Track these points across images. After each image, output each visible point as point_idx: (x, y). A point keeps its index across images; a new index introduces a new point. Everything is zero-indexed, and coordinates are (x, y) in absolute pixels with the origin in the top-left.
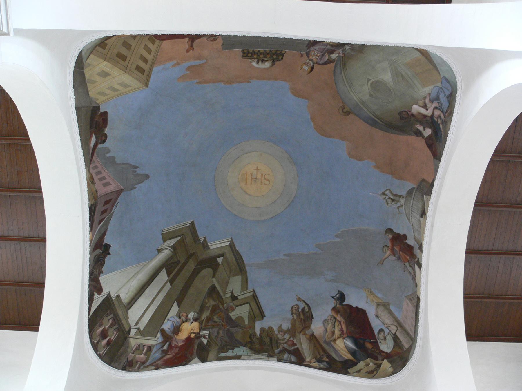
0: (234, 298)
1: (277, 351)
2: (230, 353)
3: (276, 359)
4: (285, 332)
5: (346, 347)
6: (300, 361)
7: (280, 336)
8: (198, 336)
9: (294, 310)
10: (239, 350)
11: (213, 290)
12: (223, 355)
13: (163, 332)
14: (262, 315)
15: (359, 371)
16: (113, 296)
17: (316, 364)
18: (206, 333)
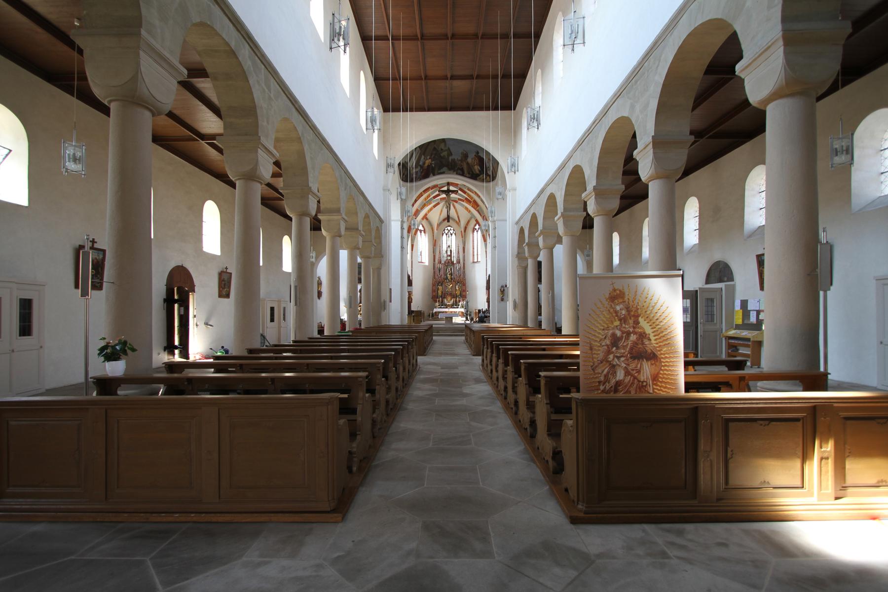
0: (442, 150)
1: (456, 169)
2: (442, 171)
3: (455, 173)
4: (460, 160)
5: (478, 169)
6: (463, 175)
7: (457, 162)
8: (431, 164)
9: (462, 153)
10: (445, 169)
11: (435, 148)
12: (439, 171)
13: (420, 166)
14: (452, 154)
15: (480, 179)
16: (404, 162)
17: (467, 175)
18: (433, 162)
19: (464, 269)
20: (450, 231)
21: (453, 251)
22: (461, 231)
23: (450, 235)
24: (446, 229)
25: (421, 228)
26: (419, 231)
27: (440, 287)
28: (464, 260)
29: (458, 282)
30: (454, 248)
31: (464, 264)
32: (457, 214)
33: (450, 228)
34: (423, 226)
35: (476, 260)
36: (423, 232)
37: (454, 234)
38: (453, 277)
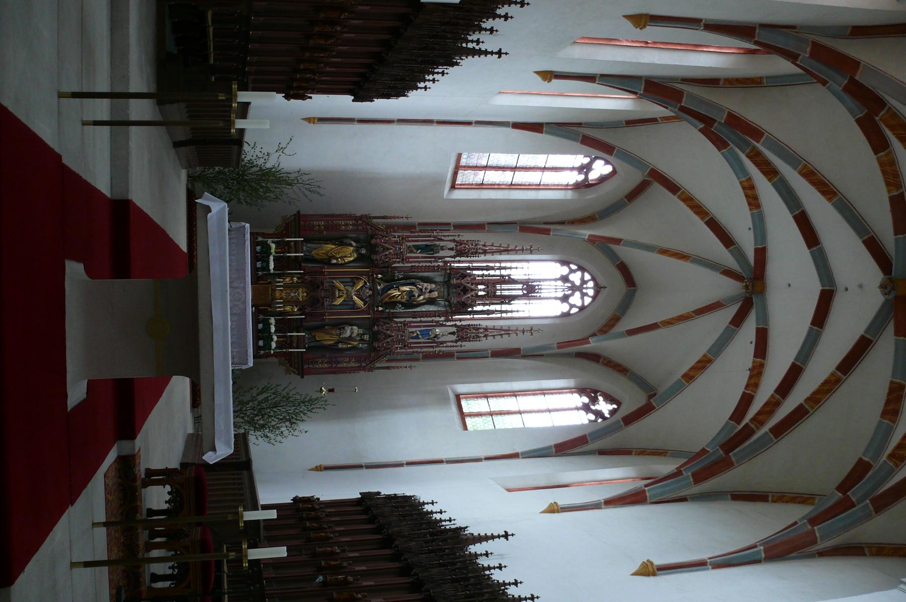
19: (428, 357)
20: (578, 294)
21: (505, 307)
22: (585, 340)
23: (560, 294)
24: (587, 277)
25: (601, 169)
26: (587, 160)
27: (349, 254)
28: (465, 356)
29: (375, 337)
30: (523, 309)
31: (449, 356)
32: (669, 323)
33: (591, 292)
34: (603, 179)
35: (468, 406)
36: (581, 177)
37: (565, 308)
38: (400, 309)
